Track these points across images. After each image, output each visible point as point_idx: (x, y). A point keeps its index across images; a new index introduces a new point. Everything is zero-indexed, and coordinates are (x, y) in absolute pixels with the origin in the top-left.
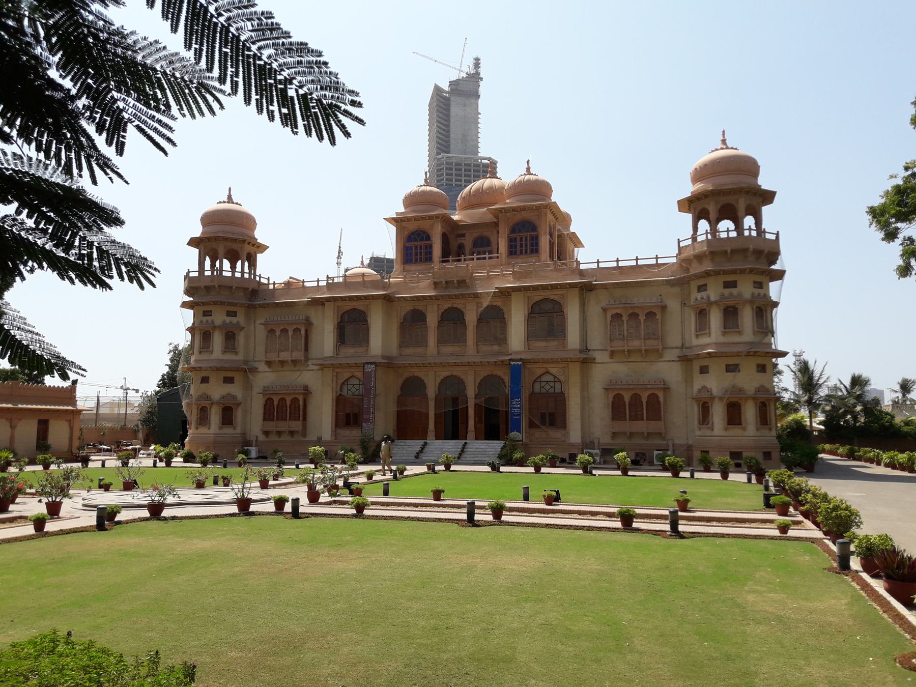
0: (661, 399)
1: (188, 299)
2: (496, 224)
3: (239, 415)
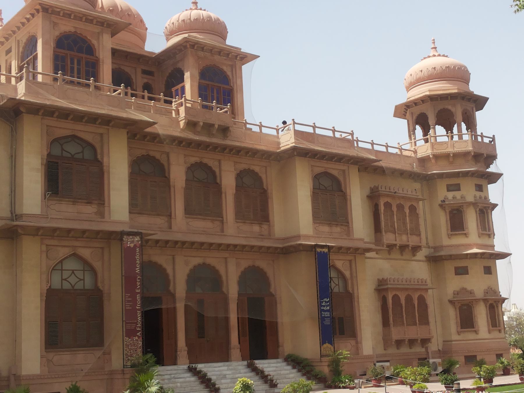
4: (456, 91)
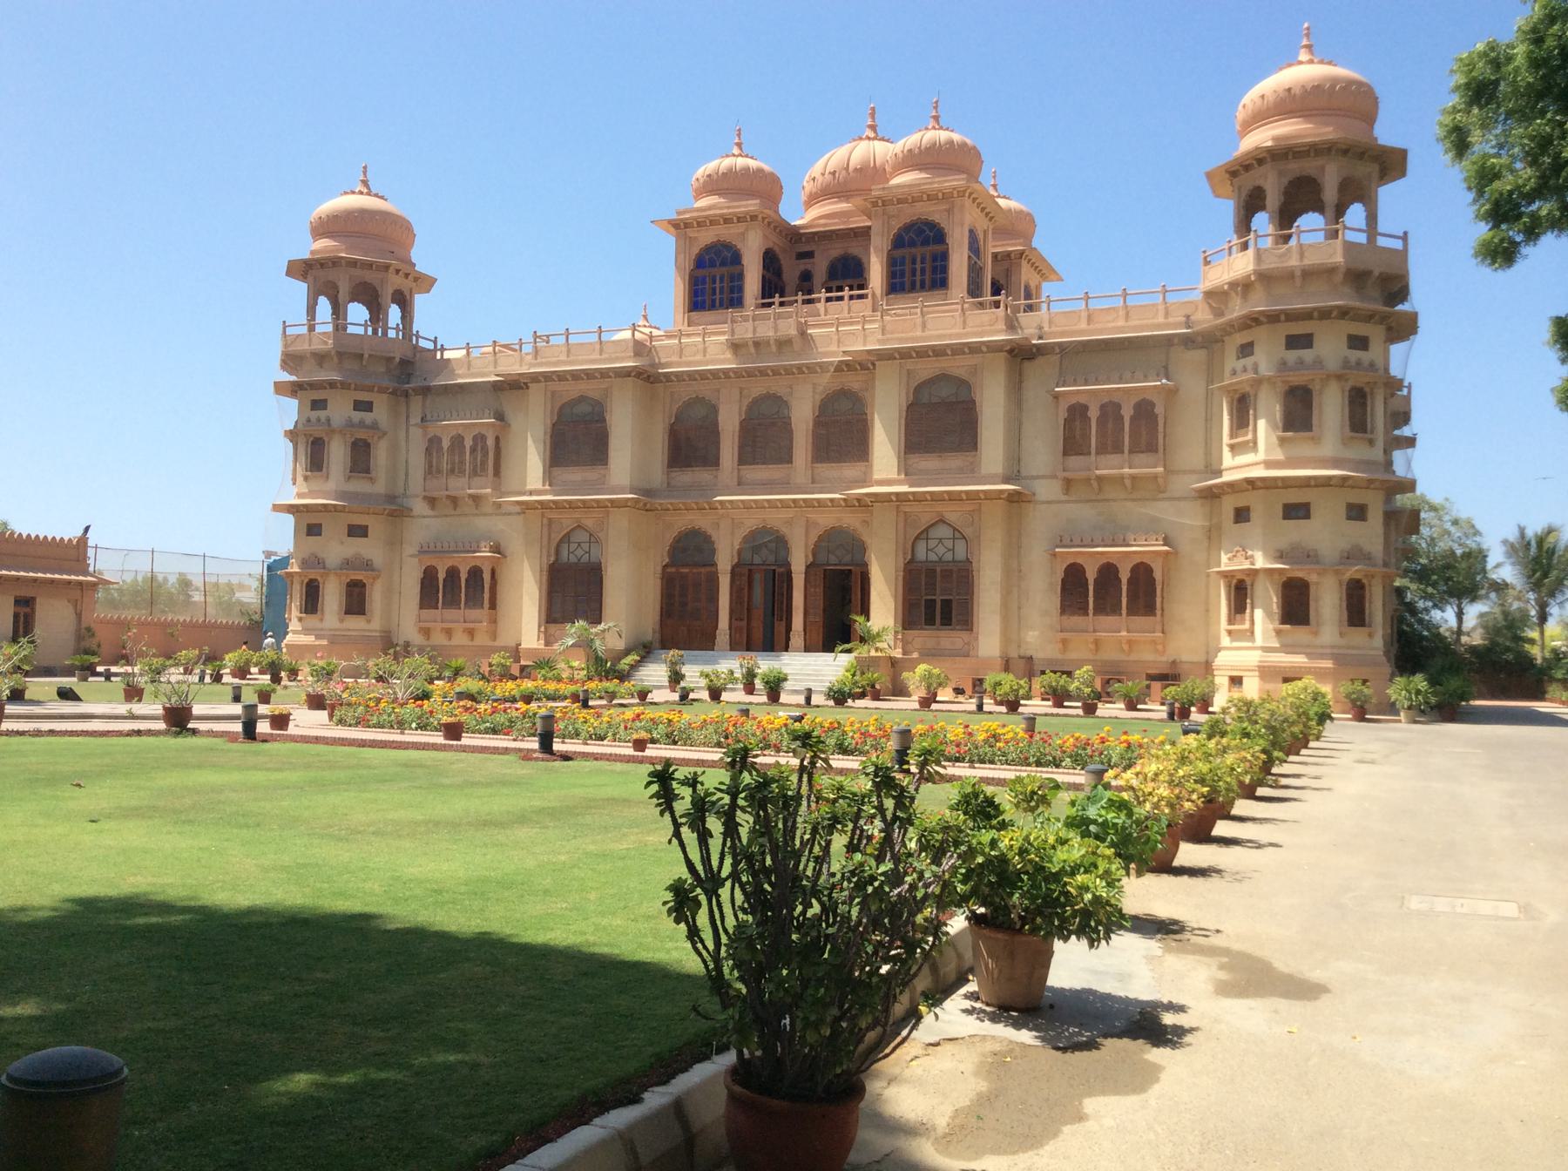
0: (1158, 575)
1: (287, 377)
2: (864, 233)
3: (376, 597)
4: (1269, 144)
